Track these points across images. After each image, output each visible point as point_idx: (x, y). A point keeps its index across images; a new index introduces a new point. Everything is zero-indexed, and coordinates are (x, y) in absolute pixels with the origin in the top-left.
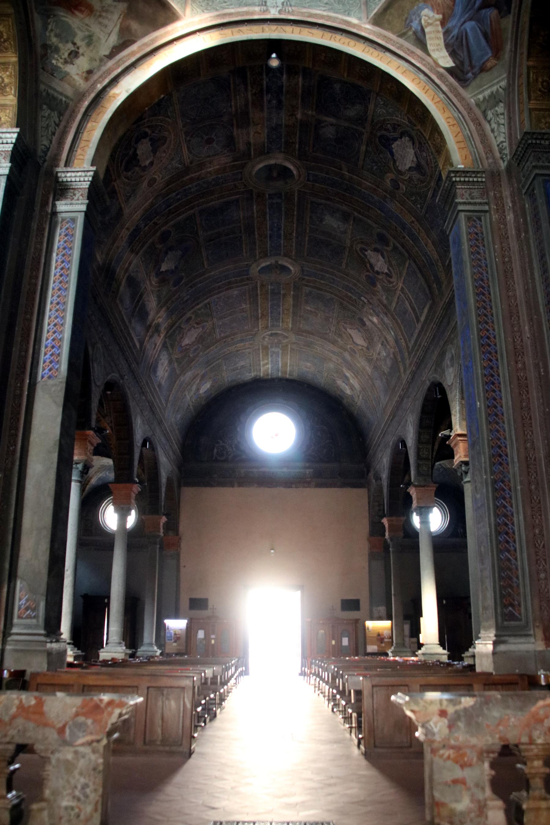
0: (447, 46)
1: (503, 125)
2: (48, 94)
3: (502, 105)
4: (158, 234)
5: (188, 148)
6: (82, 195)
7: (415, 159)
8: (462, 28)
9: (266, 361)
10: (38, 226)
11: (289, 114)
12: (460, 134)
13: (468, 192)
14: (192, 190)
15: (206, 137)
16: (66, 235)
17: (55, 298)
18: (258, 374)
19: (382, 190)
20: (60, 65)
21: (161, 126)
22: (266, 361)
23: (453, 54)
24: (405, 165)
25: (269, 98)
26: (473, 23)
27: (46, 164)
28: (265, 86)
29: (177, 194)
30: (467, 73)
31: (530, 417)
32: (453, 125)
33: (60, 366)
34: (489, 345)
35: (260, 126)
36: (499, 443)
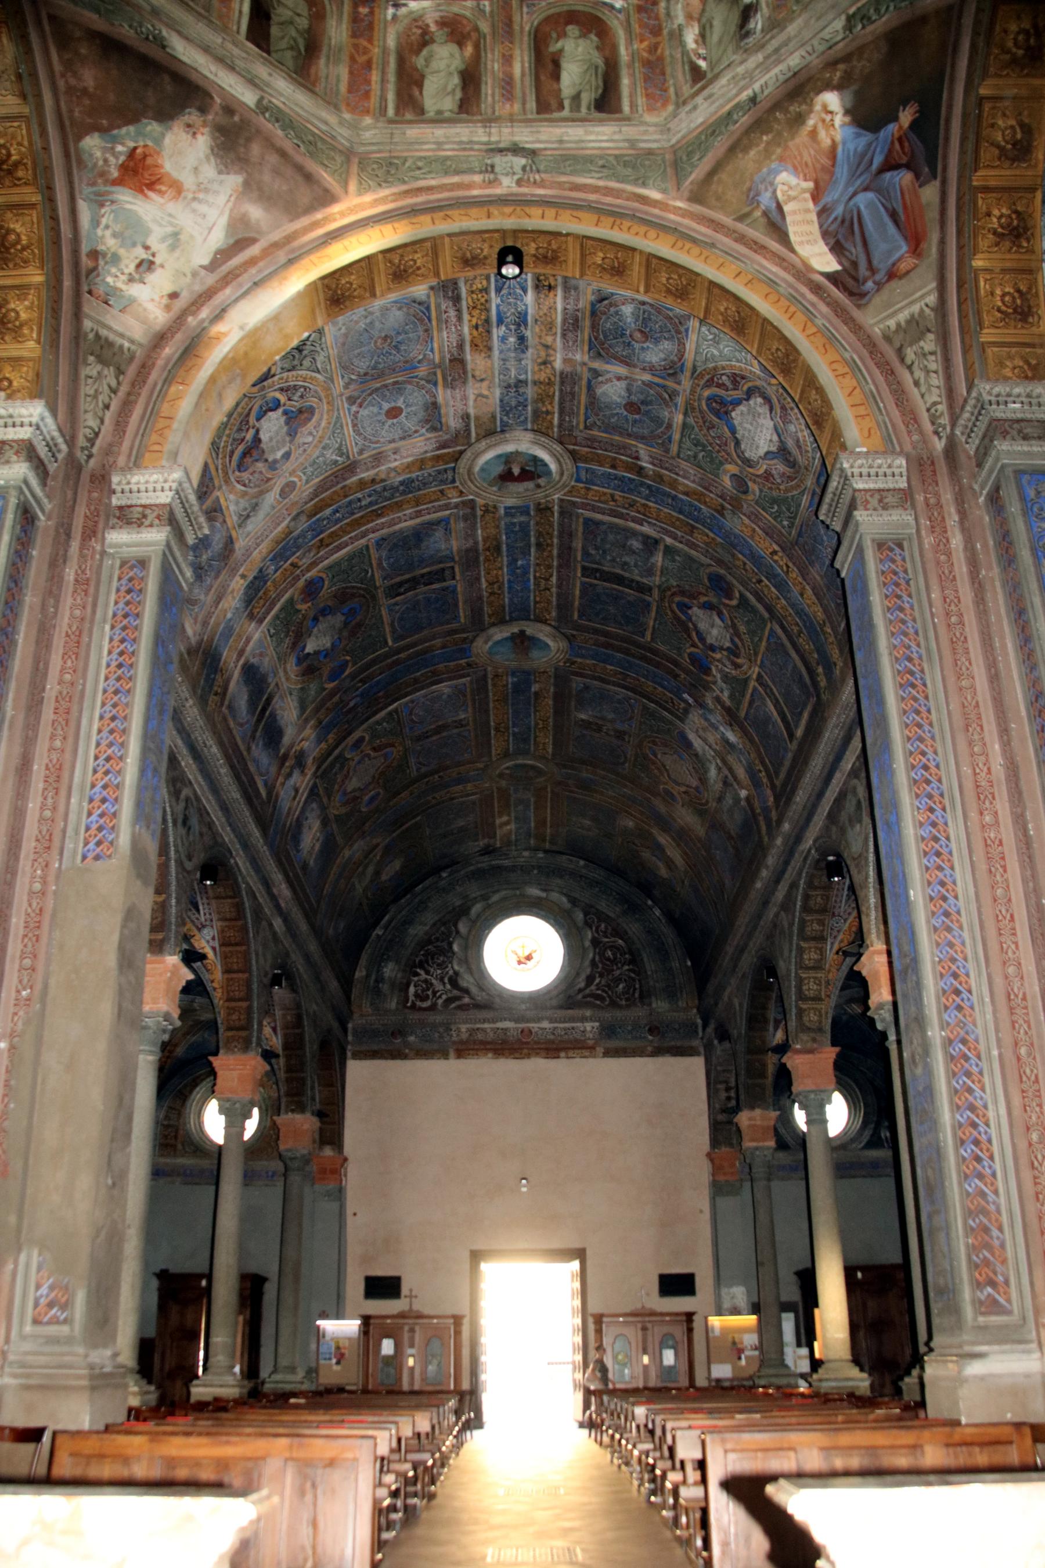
0: (825, 235)
1: (935, 372)
2: (98, 336)
3: (931, 336)
4: (301, 583)
6: (158, 517)
7: (775, 438)
8: (852, 203)
9: (505, 818)
10: (76, 573)
12: (858, 390)
13: (877, 496)
14: (363, 503)
15: (386, 406)
16: (129, 591)
17: (108, 708)
18: (492, 841)
20: (120, 285)
21: (305, 388)
22: (505, 818)
23: (837, 249)
24: (758, 447)
25: (501, 333)
26: (870, 195)
27: (92, 462)
30: (864, 284)
31: (1012, 916)
32: (843, 375)
33: (117, 837)
34: (928, 782)
36: (954, 967)
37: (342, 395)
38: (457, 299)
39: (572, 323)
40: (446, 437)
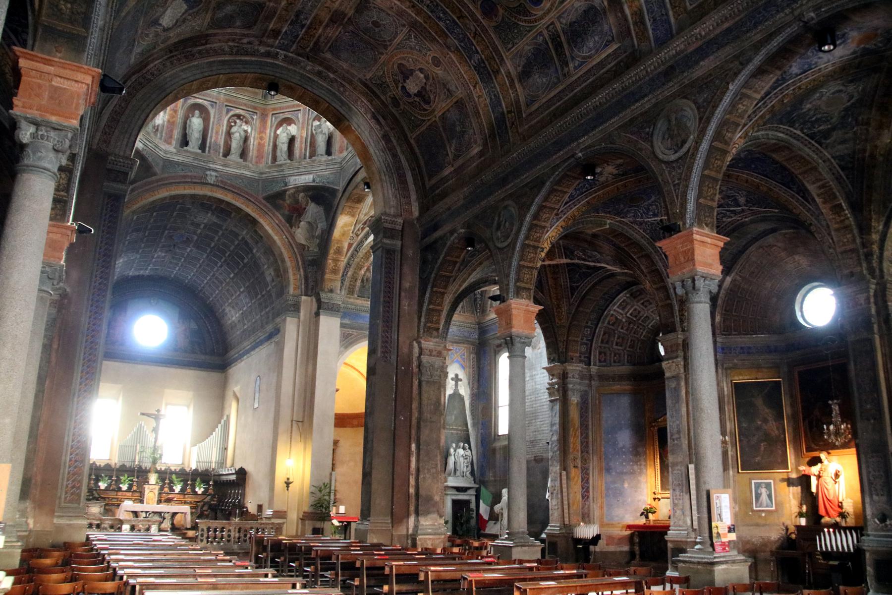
5: (395, 38)
15: (377, 30)
28: (304, 30)
29: (439, 18)
38: (316, 43)
39: (268, 18)
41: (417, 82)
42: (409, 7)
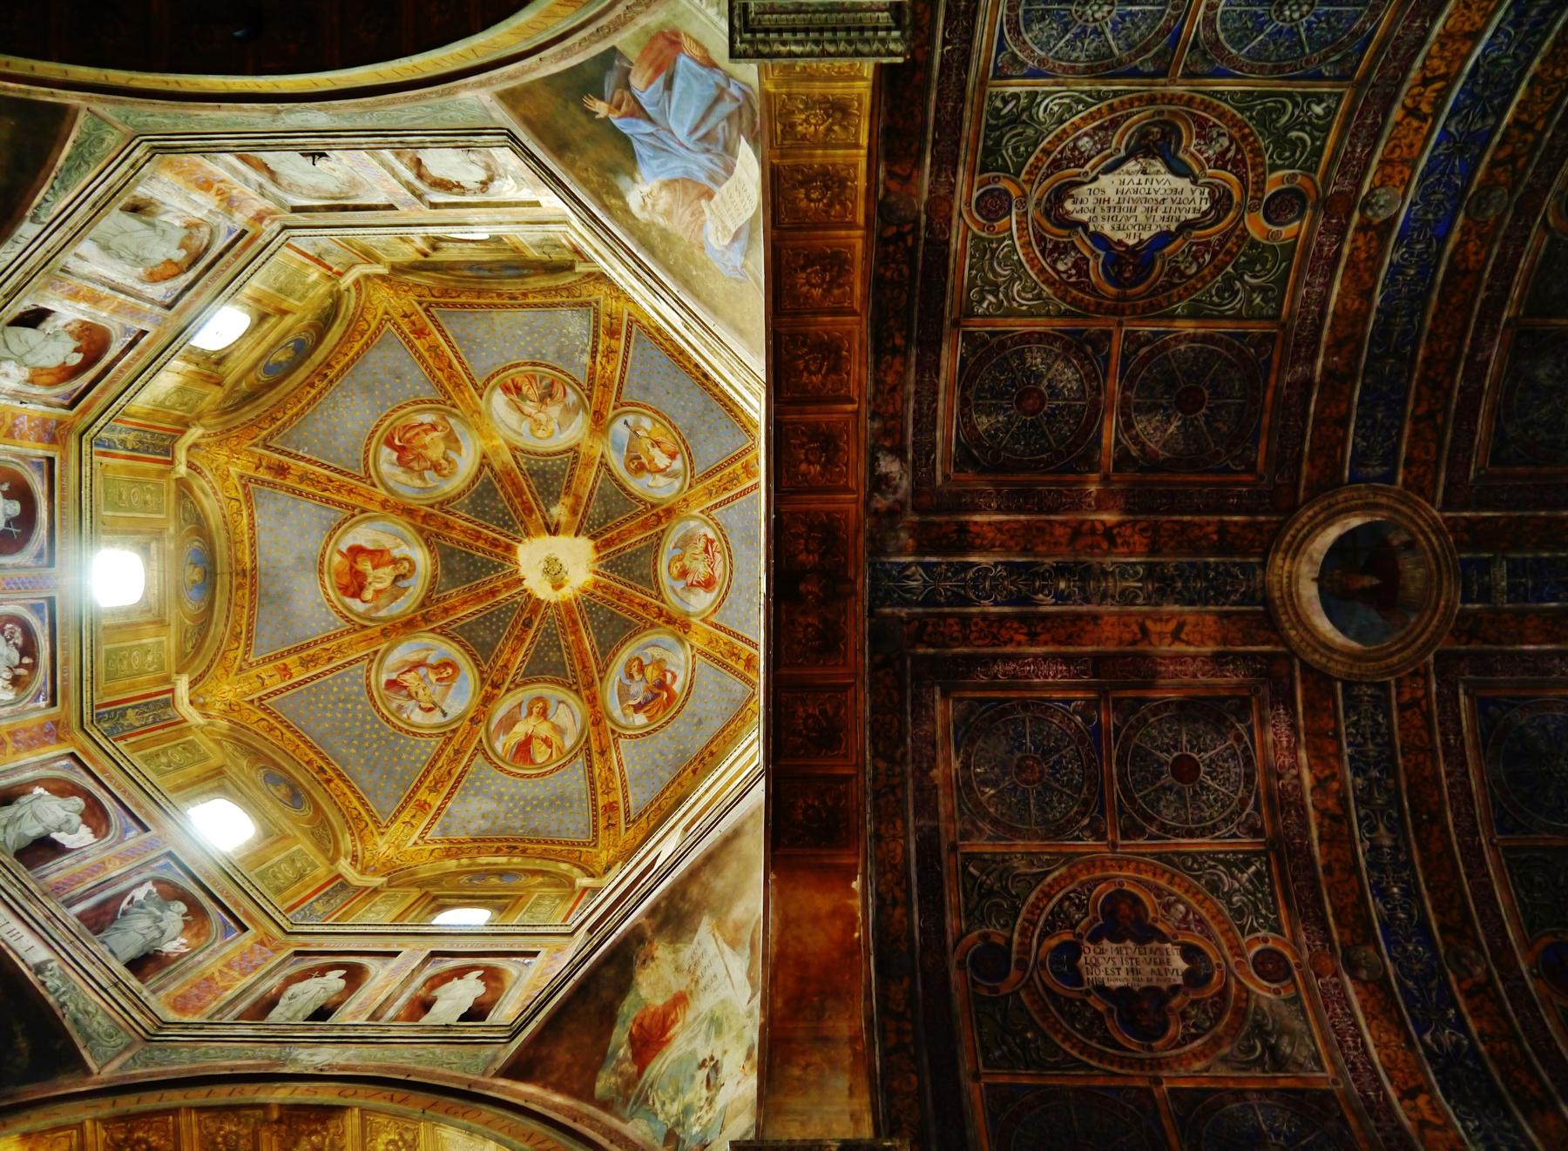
7: (1131, 165)
11: (1105, 545)
15: (1167, 779)
19: (1342, 240)
21: (1066, 897)
25: (1050, 600)
28: (1007, 609)
29: (1382, 893)
35: (1149, 624)
37: (1114, 845)
38: (973, 661)
40: (1265, 691)
41: (1146, 969)
42: (1323, 813)
